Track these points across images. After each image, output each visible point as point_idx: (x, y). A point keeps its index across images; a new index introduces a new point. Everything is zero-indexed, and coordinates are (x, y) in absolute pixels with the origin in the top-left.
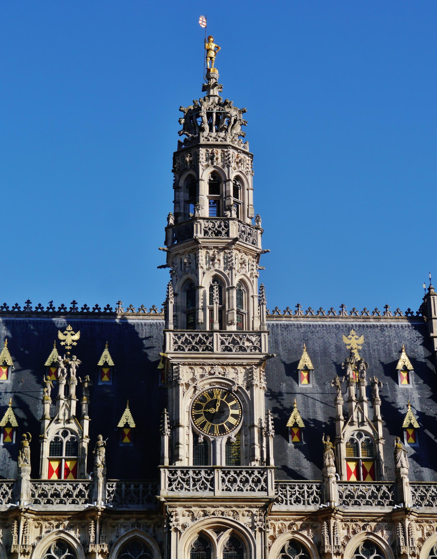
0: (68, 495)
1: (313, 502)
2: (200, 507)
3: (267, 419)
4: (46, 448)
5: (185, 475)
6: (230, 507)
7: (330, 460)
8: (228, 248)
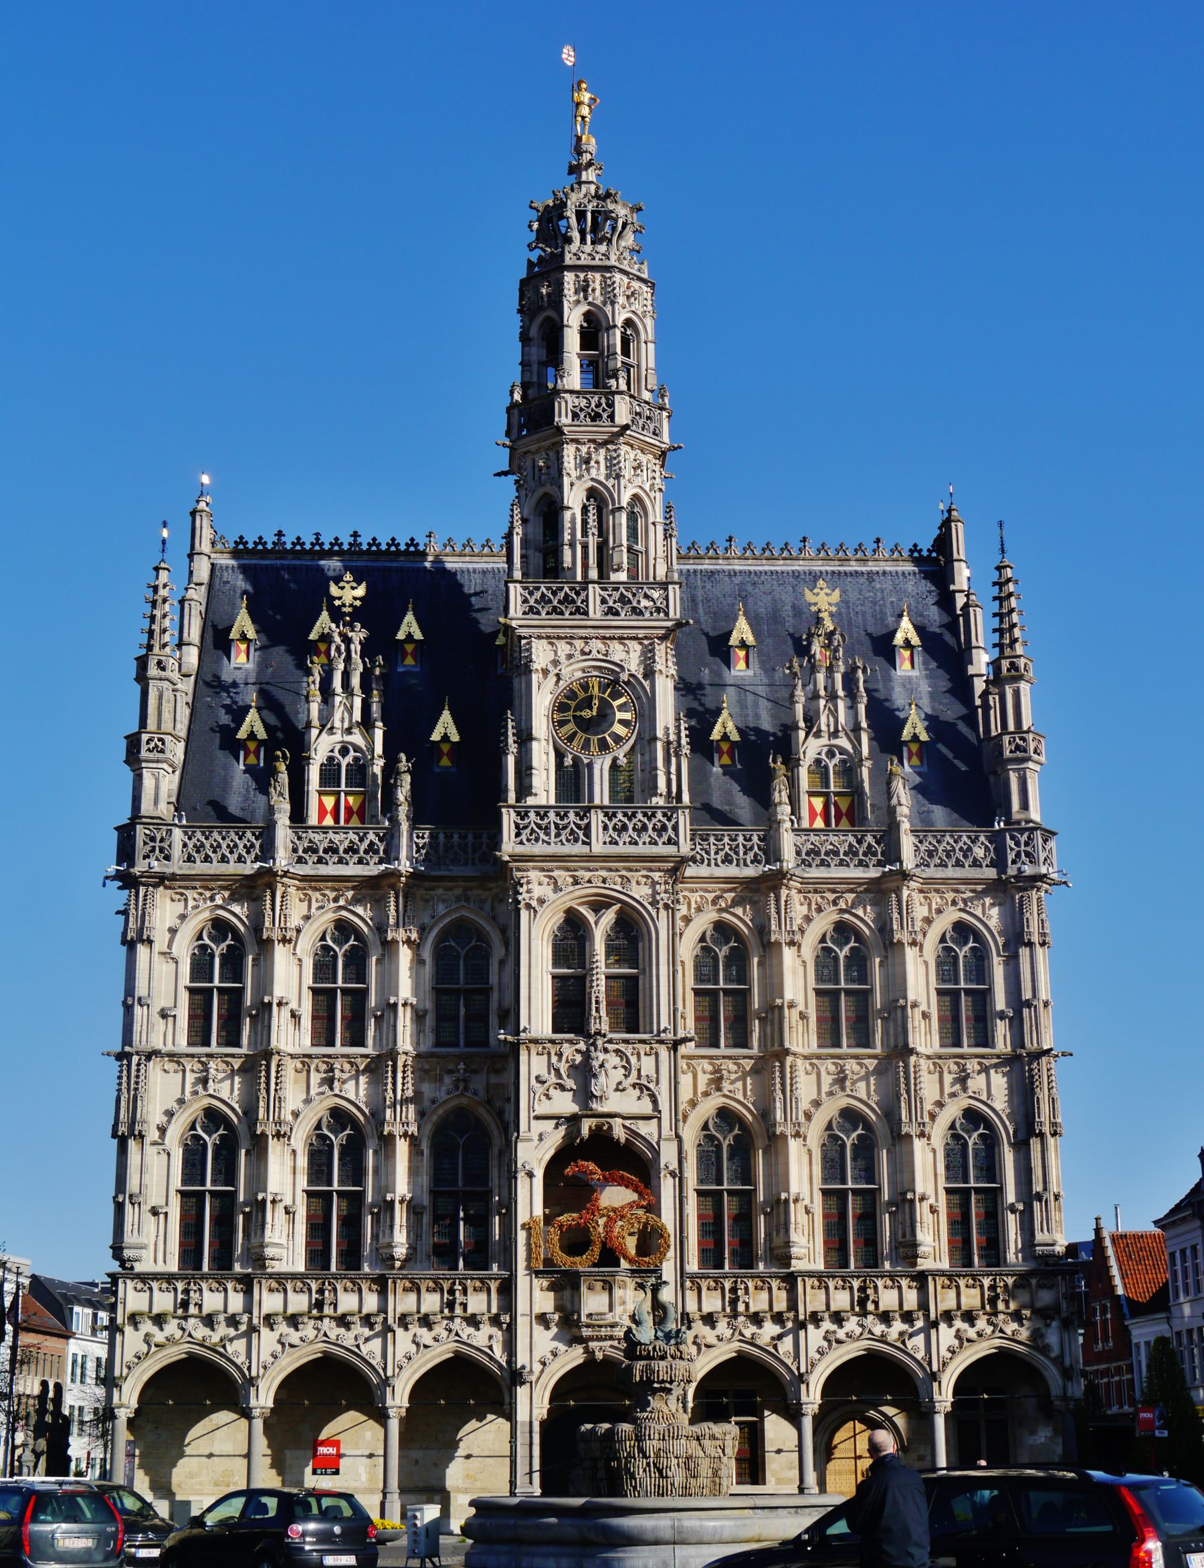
0: (351, 849)
1: (752, 862)
2: (568, 870)
3: (678, 727)
4: (314, 775)
5: (542, 819)
6: (617, 870)
7: (781, 795)
8: (612, 443)
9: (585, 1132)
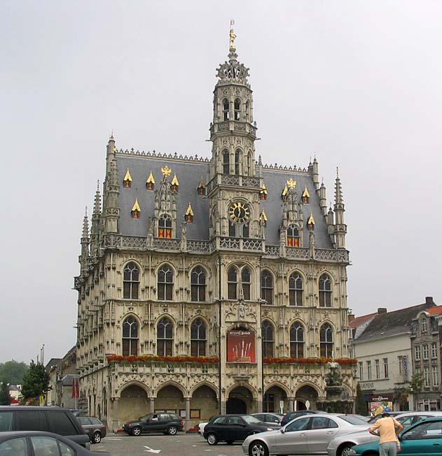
9: (238, 326)
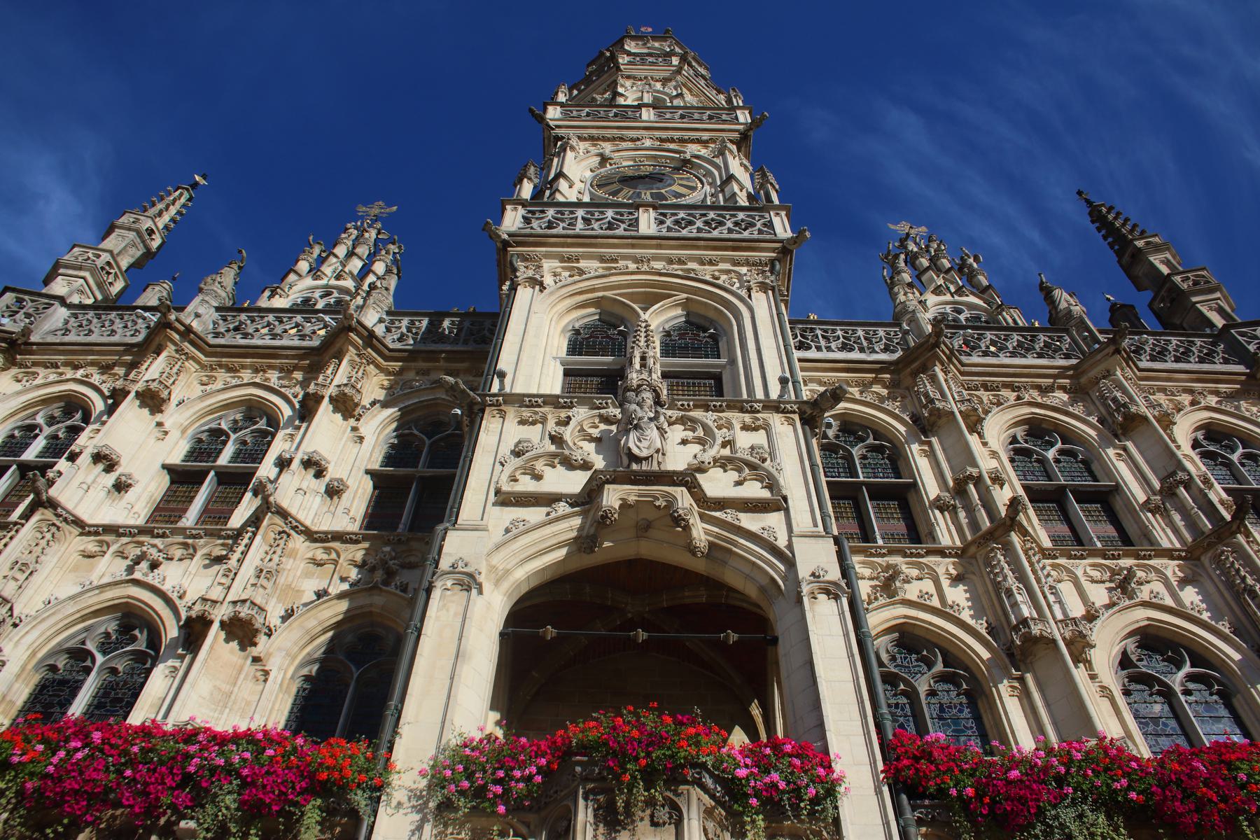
6: (681, 262)
